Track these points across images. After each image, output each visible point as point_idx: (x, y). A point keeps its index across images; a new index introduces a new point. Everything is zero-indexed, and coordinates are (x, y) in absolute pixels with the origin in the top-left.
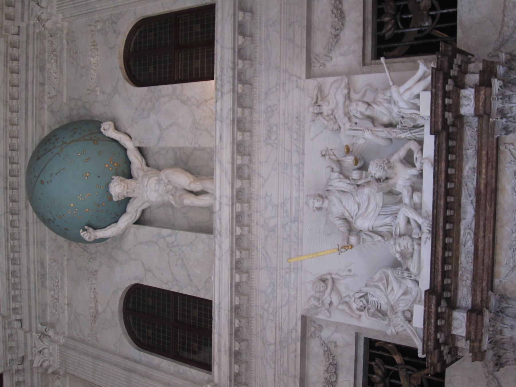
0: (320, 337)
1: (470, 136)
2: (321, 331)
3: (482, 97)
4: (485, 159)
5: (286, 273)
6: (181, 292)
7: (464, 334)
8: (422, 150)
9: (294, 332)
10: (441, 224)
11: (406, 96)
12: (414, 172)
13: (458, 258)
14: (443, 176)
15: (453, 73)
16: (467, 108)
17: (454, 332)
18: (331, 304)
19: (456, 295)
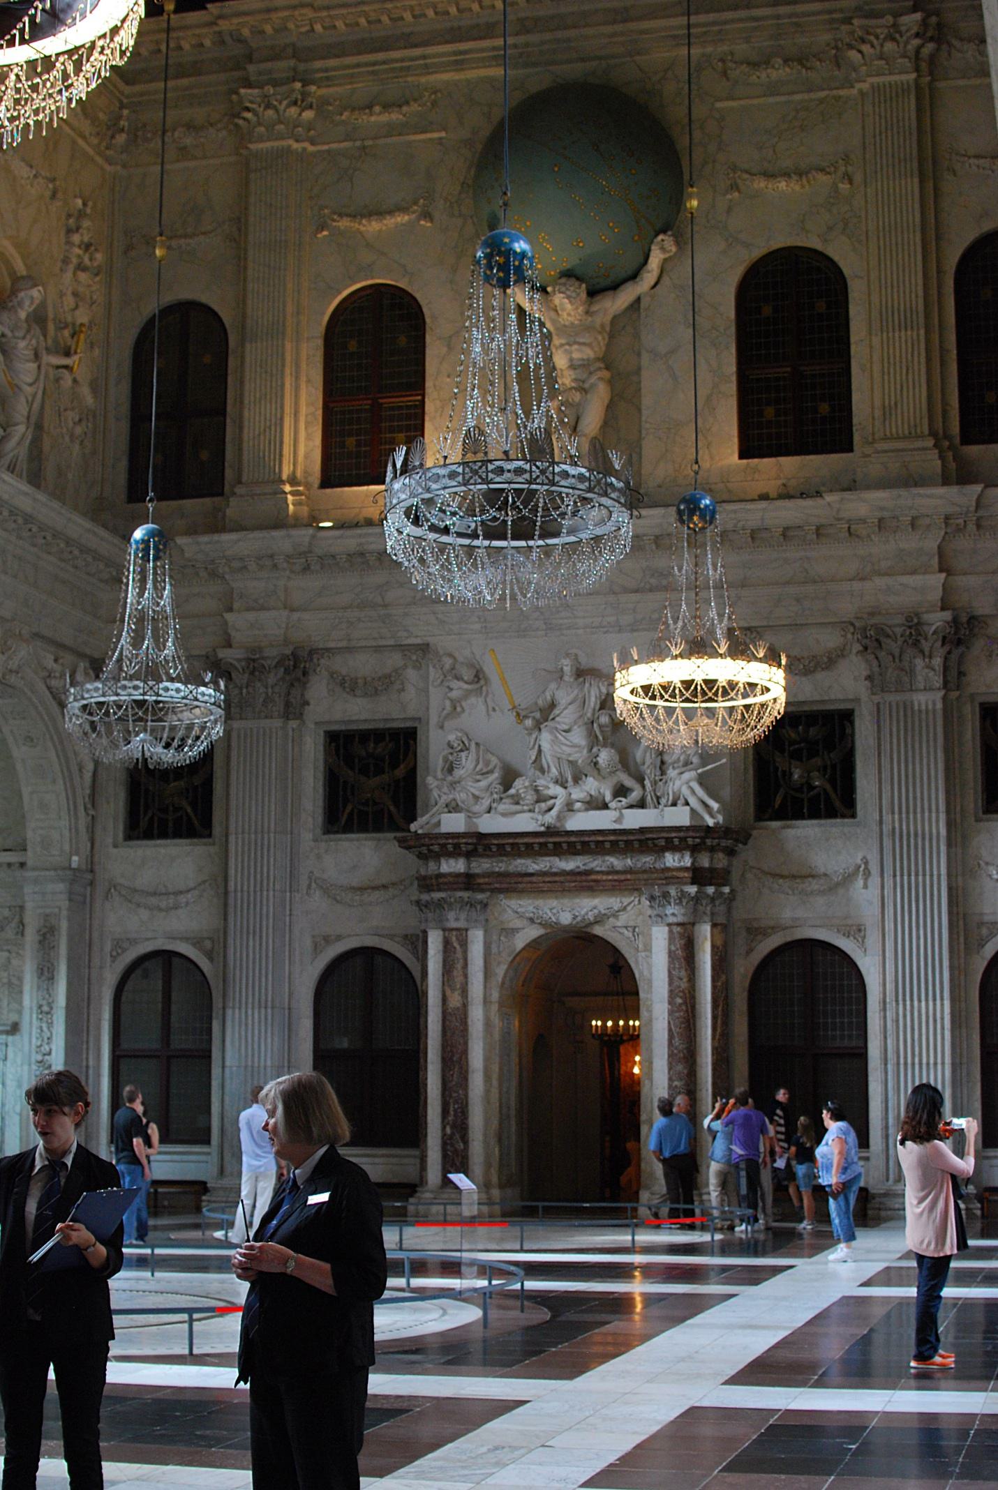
0: (405, 666)
1: (647, 860)
2: (414, 667)
3: (681, 874)
4: (622, 877)
5: (479, 618)
6: (427, 418)
7: (442, 871)
8: (631, 807)
9: (405, 634)
10: (551, 840)
11: (685, 791)
12: (608, 797)
13: (520, 855)
14: (601, 839)
15: (709, 842)
16: (671, 860)
17: (443, 861)
18: (451, 689)
19: (481, 856)
